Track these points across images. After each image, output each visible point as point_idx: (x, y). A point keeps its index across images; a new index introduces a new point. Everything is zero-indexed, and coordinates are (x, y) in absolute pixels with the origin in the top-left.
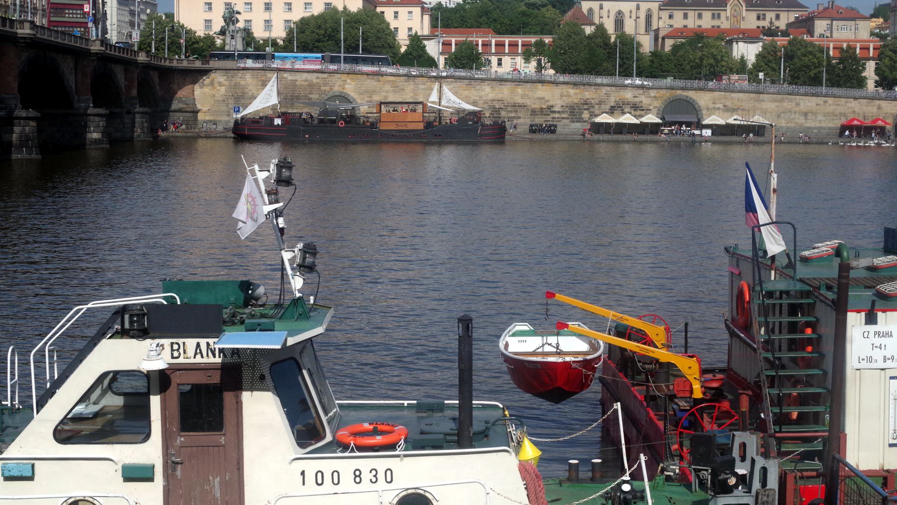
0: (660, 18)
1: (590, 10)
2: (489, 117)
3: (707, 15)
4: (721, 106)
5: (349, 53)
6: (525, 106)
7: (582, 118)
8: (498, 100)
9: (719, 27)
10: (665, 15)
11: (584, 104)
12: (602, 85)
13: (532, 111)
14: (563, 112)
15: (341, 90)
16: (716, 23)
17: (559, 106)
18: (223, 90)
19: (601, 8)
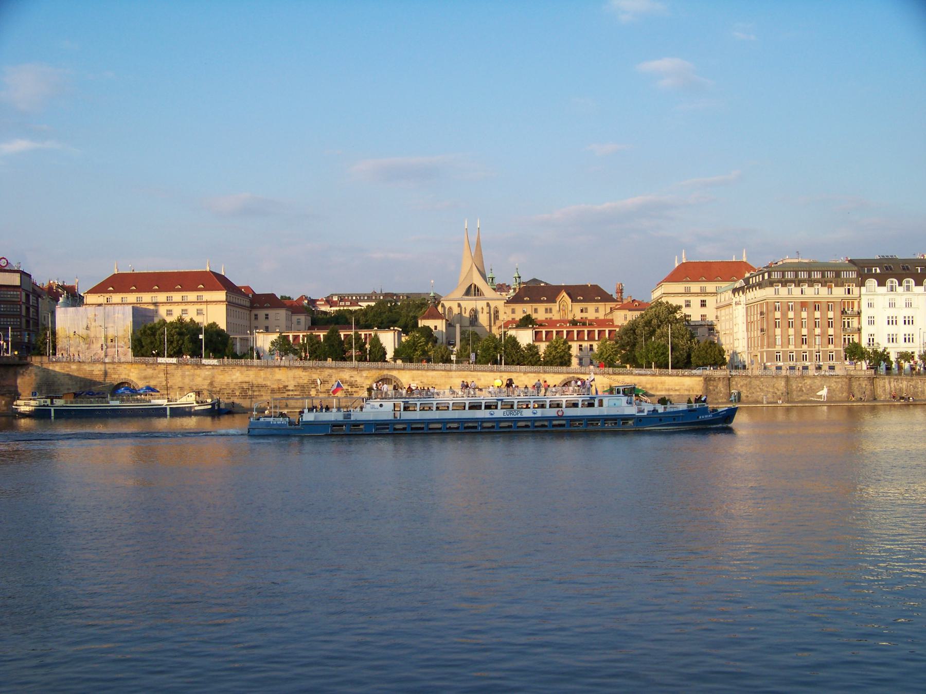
2: (239, 396)
3: (541, 307)
6: (266, 386)
7: (311, 395)
8: (246, 382)
9: (551, 318)
11: (311, 384)
13: (272, 390)
14: (295, 390)
15: (127, 377)
16: (549, 316)
17: (293, 385)
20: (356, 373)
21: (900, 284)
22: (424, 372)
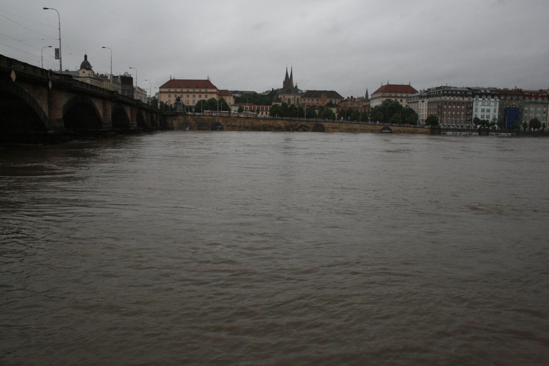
0: (301, 100)
1: (281, 98)
4: (330, 127)
5: (221, 109)
10: (303, 100)
12: (297, 120)
18: (182, 121)
19: (284, 97)
20: (307, 122)
21: (487, 98)
22: (333, 123)
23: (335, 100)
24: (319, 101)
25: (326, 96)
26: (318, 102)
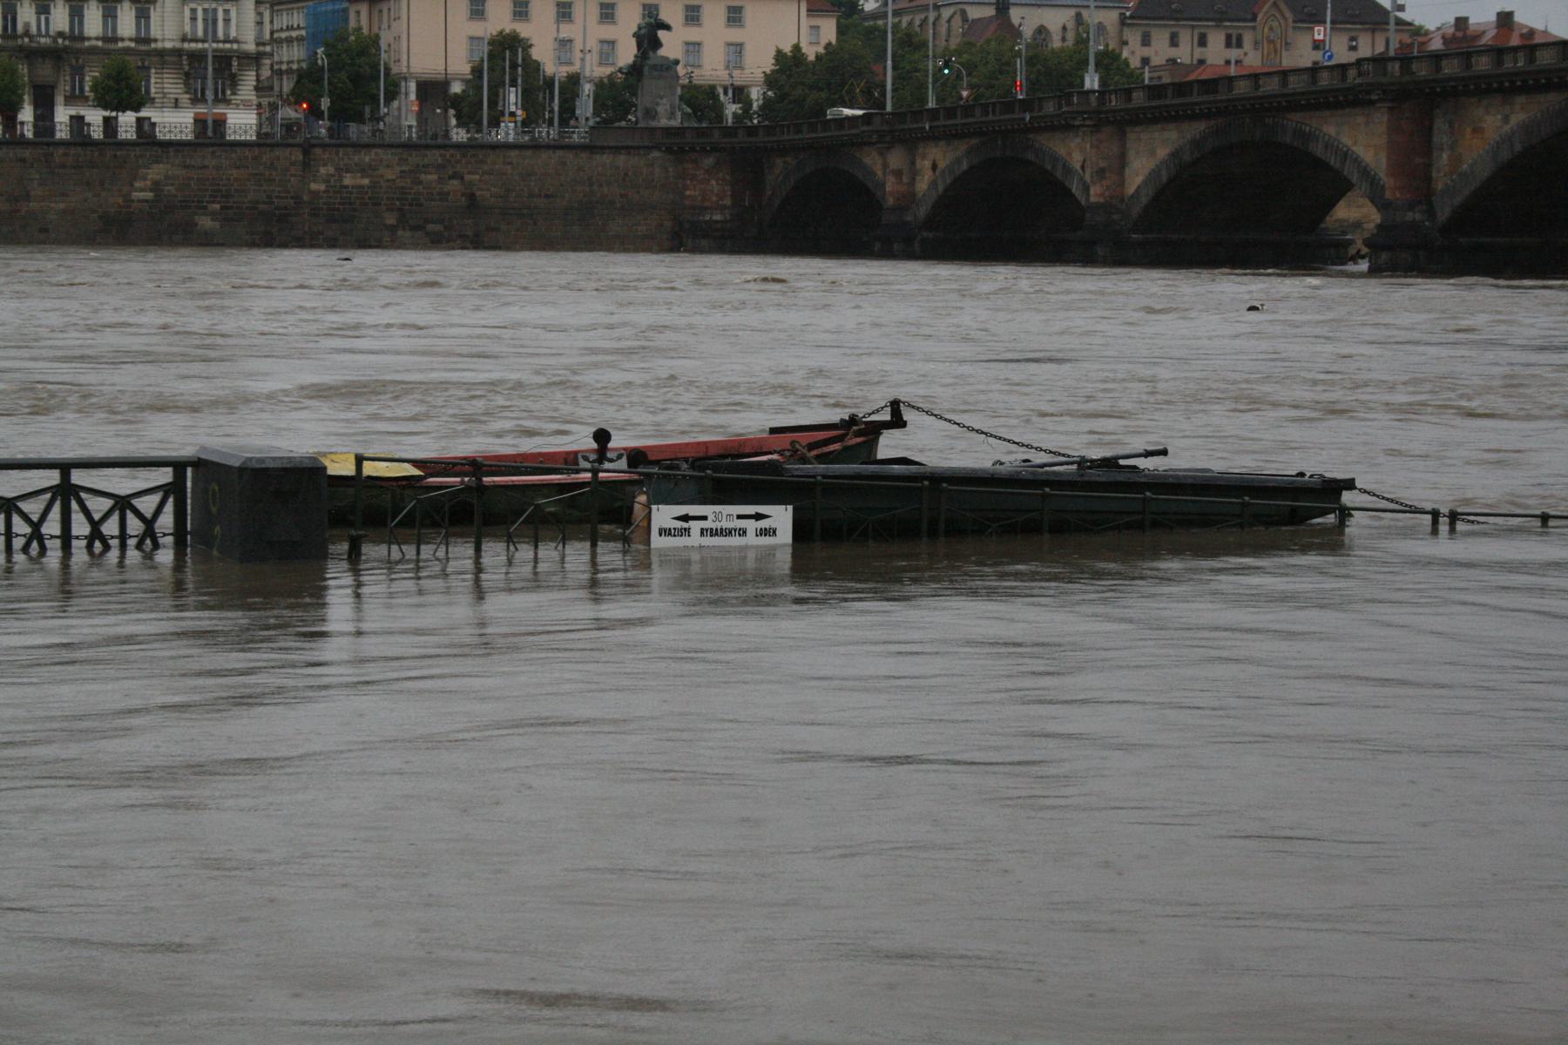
0: (1126, 43)
10: (1134, 37)
23: (1352, 39)
24: (1239, 45)
25: (1288, 14)
26: (1234, 54)
